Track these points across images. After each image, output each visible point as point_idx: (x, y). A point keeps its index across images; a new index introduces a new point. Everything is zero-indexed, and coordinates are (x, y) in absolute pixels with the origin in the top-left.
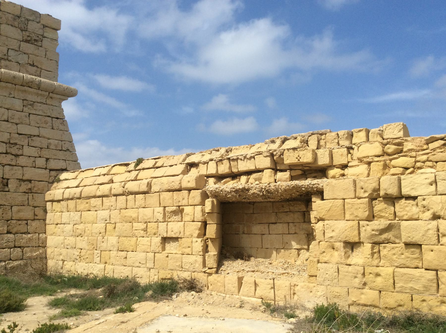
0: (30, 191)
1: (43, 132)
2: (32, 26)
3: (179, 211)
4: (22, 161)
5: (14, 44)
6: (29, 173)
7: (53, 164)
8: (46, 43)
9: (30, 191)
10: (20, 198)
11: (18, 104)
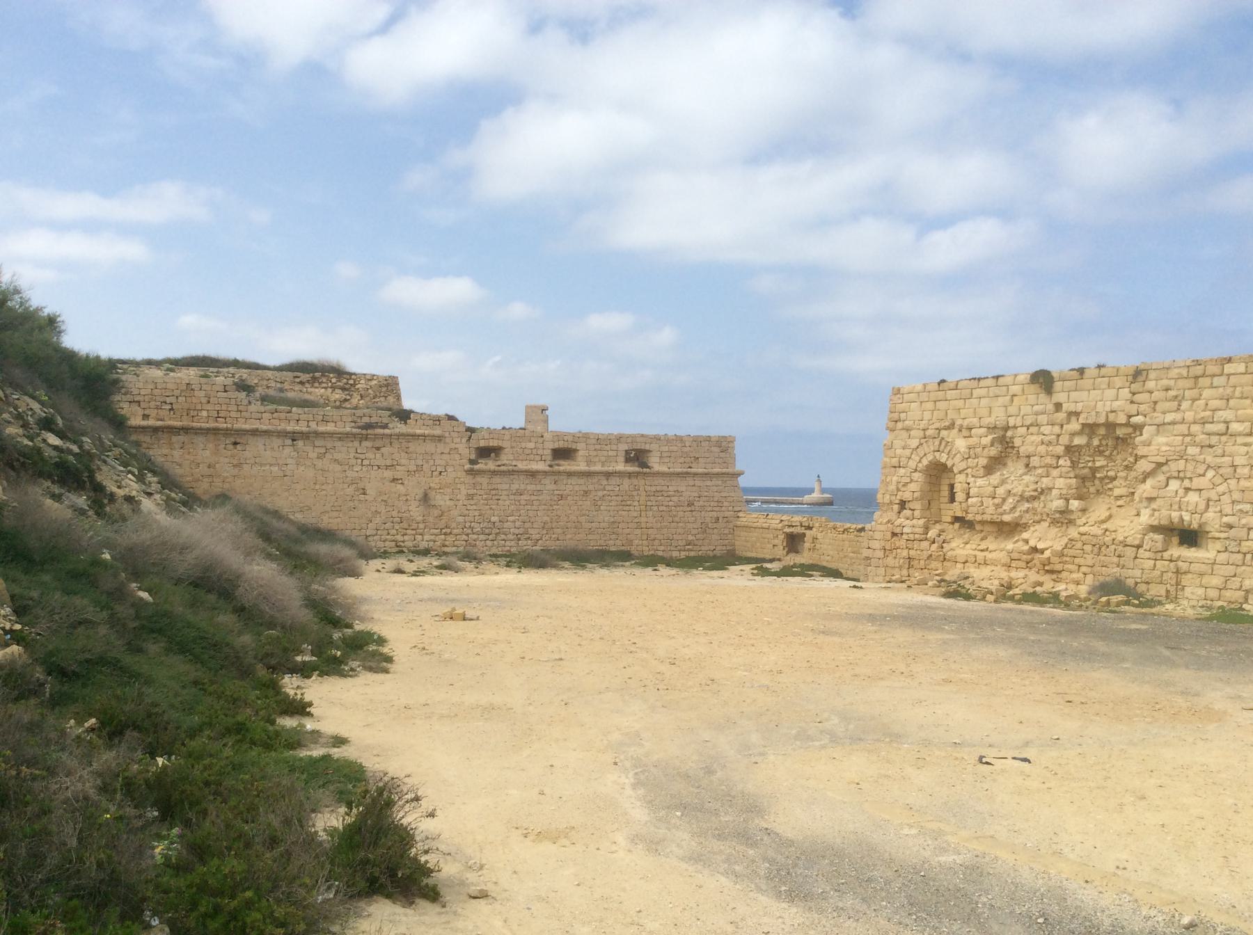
0: (727, 522)
1: (732, 494)
2: (724, 444)
3: (777, 536)
4: (723, 509)
5: (717, 455)
6: (727, 514)
7: (736, 509)
8: (729, 451)
9: (727, 522)
10: (724, 525)
11: (720, 482)
